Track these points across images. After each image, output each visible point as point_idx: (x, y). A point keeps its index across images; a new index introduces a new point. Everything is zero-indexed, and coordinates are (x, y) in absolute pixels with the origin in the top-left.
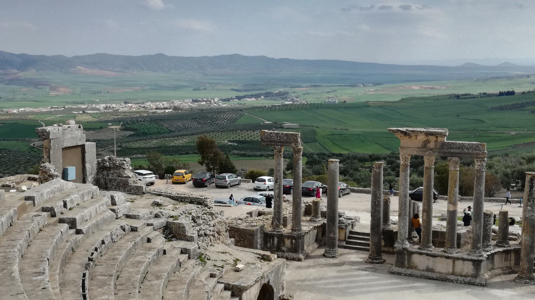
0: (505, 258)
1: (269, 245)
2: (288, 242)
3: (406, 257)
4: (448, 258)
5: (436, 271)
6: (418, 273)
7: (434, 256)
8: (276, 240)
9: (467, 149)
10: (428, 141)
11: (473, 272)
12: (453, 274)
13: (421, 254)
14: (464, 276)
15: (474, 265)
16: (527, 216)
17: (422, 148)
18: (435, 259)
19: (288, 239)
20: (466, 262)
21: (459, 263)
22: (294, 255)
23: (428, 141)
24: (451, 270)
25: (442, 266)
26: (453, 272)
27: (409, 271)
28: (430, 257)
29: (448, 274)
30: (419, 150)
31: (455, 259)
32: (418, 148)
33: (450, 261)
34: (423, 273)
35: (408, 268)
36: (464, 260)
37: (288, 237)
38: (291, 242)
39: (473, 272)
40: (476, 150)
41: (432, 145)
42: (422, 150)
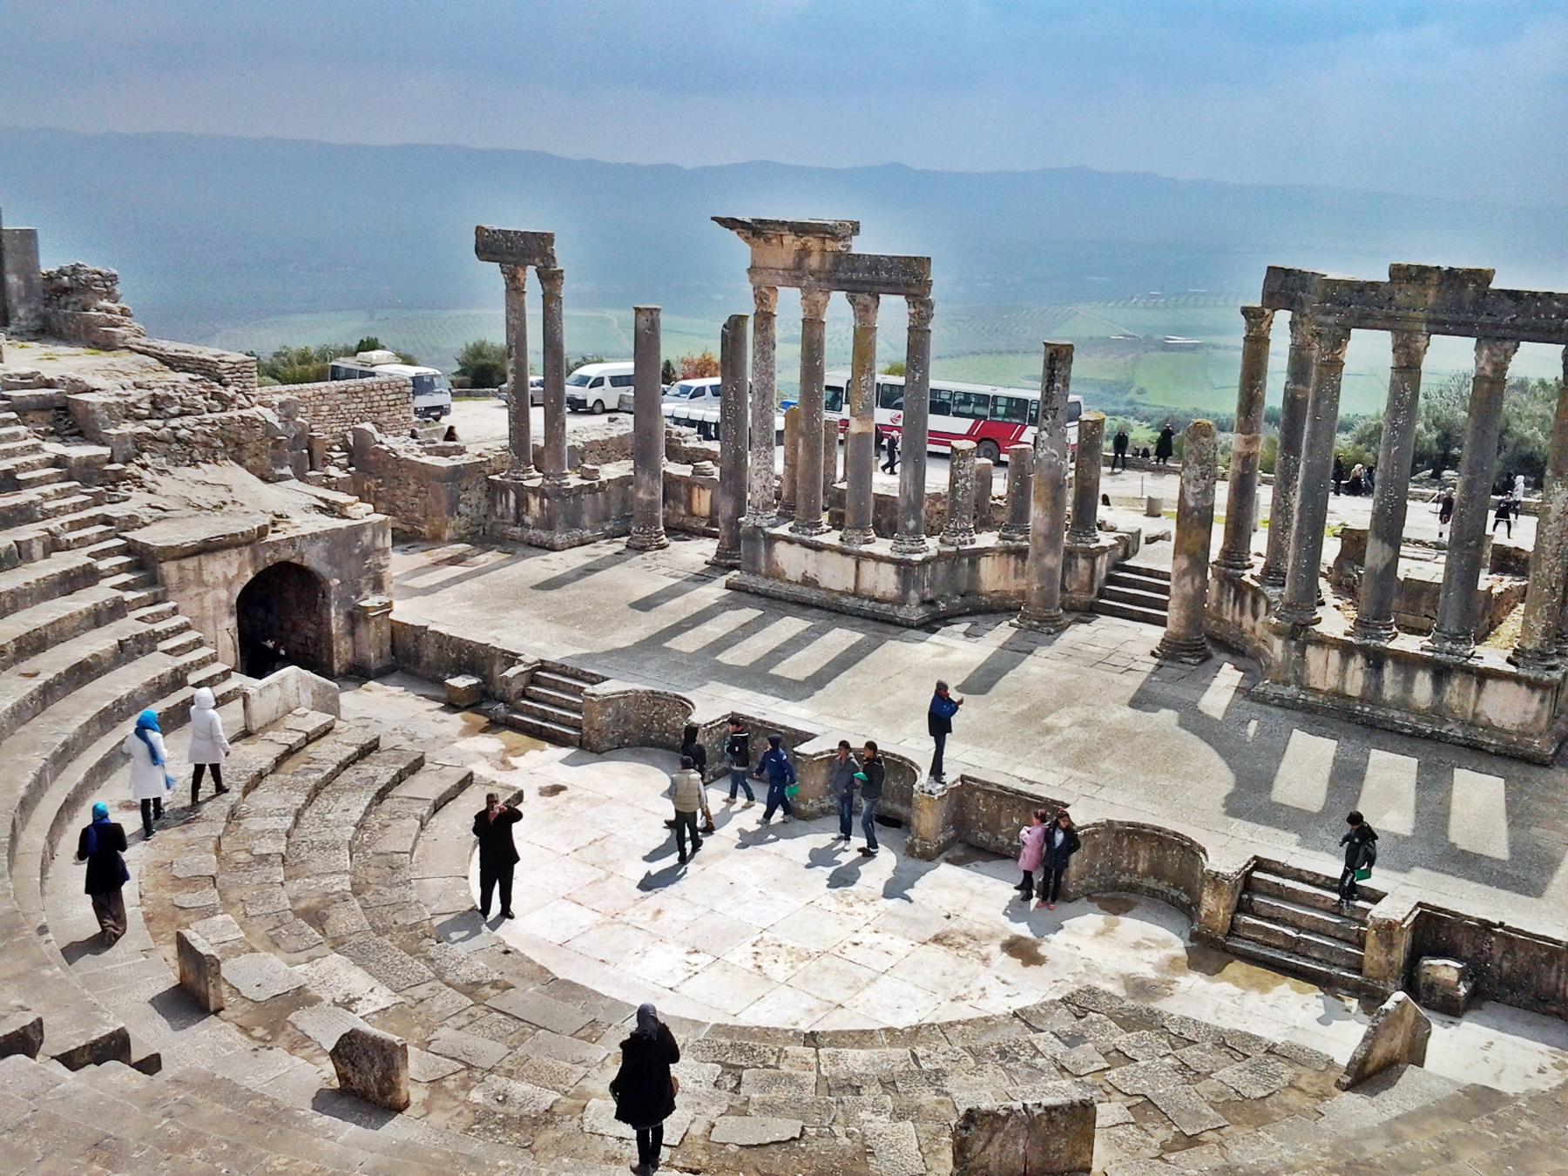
0: (1016, 570)
1: (499, 509)
2: (534, 503)
4: (844, 553)
5: (822, 585)
6: (784, 589)
7: (818, 548)
8: (512, 496)
9: (888, 271)
10: (804, 252)
12: (856, 594)
13: (790, 541)
14: (877, 600)
15: (898, 573)
18: (819, 555)
19: (535, 496)
20: (882, 565)
21: (868, 567)
22: (544, 535)
23: (804, 252)
24: (851, 585)
25: (835, 574)
27: (765, 585)
29: (842, 593)
31: (860, 557)
34: (797, 588)
35: (767, 577)
36: (879, 559)
37: (534, 490)
38: (541, 503)
41: (814, 262)
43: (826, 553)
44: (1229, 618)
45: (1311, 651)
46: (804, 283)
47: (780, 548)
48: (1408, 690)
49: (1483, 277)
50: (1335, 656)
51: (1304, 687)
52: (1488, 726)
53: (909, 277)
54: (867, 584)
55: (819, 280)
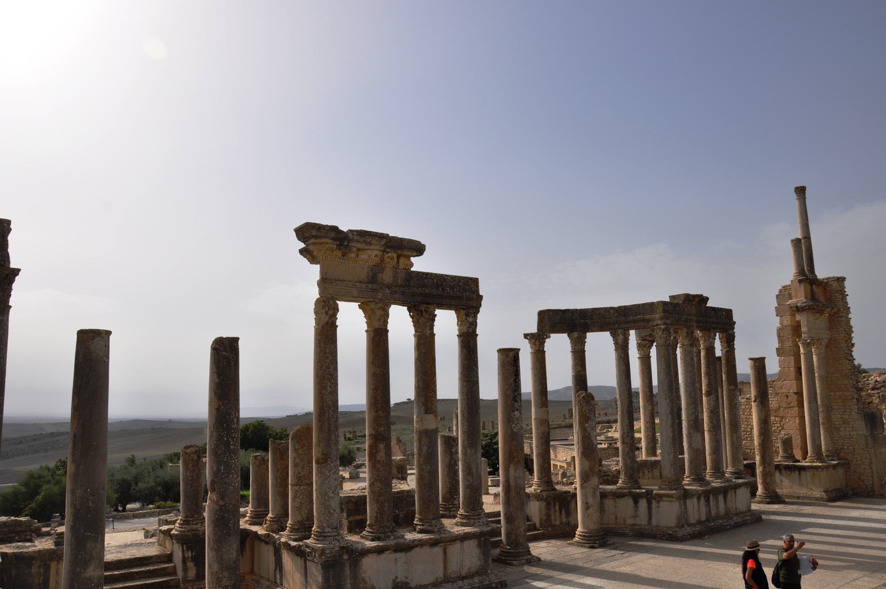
3: (347, 572)
9: (452, 288)
11: (479, 563)
13: (379, 551)
15: (479, 546)
16: (515, 430)
17: (369, 283)
21: (454, 549)
23: (377, 269)
24: (440, 574)
26: (444, 576)
28: (398, 555)
30: (364, 286)
32: (360, 282)
33: (438, 550)
39: (479, 563)
40: (465, 291)
41: (387, 276)
42: (370, 286)
43: (417, 550)
44: (558, 523)
45: (688, 501)
46: (380, 295)
47: (369, 564)
48: (718, 507)
49: (707, 299)
50: (695, 500)
51: (690, 525)
52: (741, 513)
53: (463, 295)
54: (453, 567)
55: (395, 293)
